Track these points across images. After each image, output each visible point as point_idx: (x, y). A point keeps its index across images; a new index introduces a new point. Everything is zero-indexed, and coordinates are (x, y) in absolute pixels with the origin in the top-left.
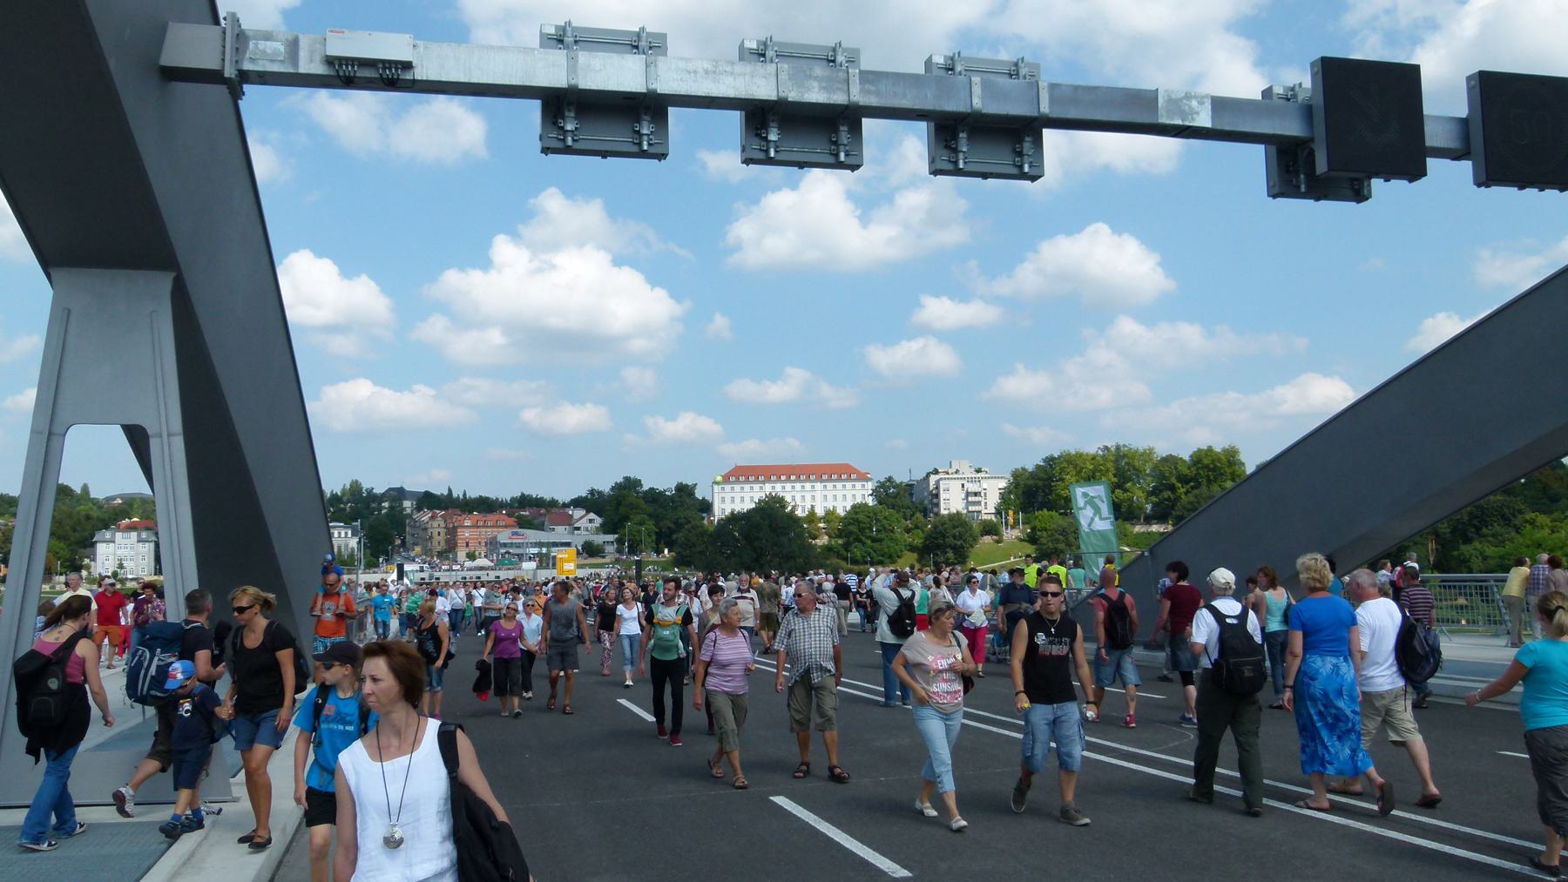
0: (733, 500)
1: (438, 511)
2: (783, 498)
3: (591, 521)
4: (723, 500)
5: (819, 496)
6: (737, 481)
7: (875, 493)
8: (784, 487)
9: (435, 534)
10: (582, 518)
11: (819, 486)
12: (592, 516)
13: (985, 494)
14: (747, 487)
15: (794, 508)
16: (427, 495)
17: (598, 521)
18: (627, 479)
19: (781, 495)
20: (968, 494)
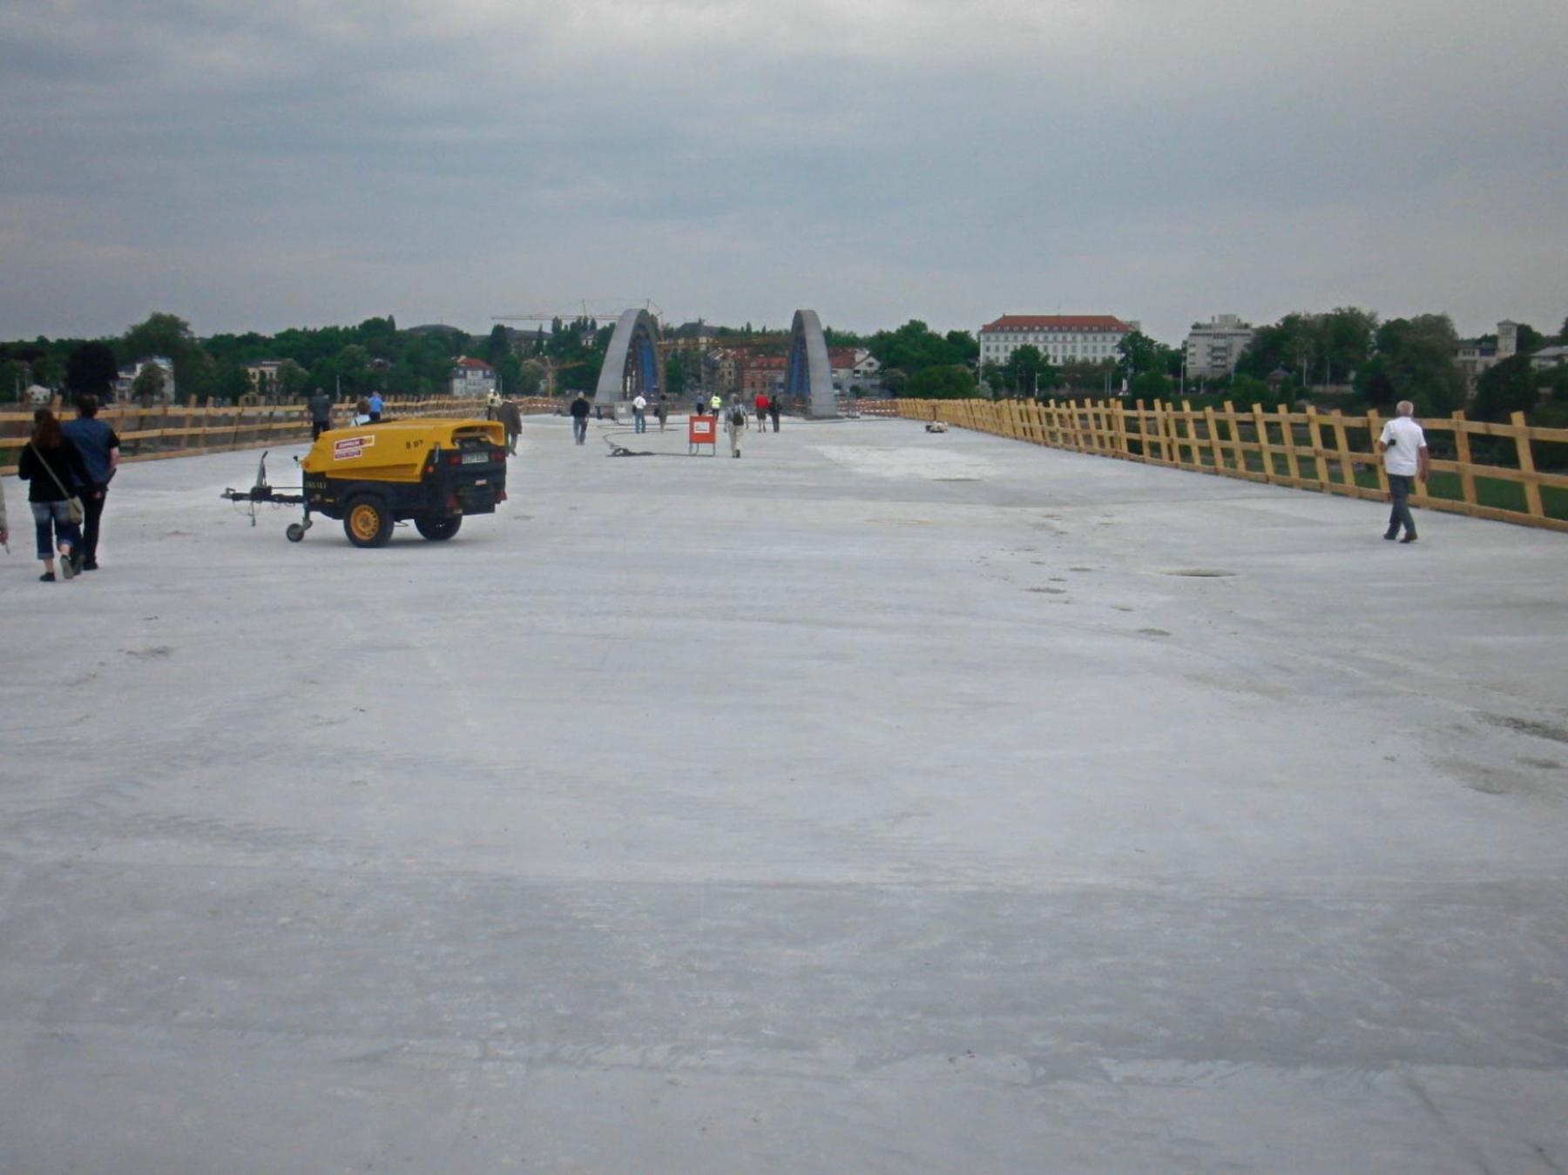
0: (997, 349)
1: (729, 351)
2: (1036, 348)
3: (870, 365)
4: (988, 349)
5: (1079, 346)
6: (1002, 330)
7: (1122, 347)
8: (1036, 338)
9: (726, 374)
10: (862, 361)
11: (1079, 337)
12: (872, 360)
13: (1231, 350)
14: (1011, 337)
15: (1047, 357)
16: (723, 332)
17: (877, 364)
18: (913, 322)
19: (1034, 345)
20: (1214, 349)
